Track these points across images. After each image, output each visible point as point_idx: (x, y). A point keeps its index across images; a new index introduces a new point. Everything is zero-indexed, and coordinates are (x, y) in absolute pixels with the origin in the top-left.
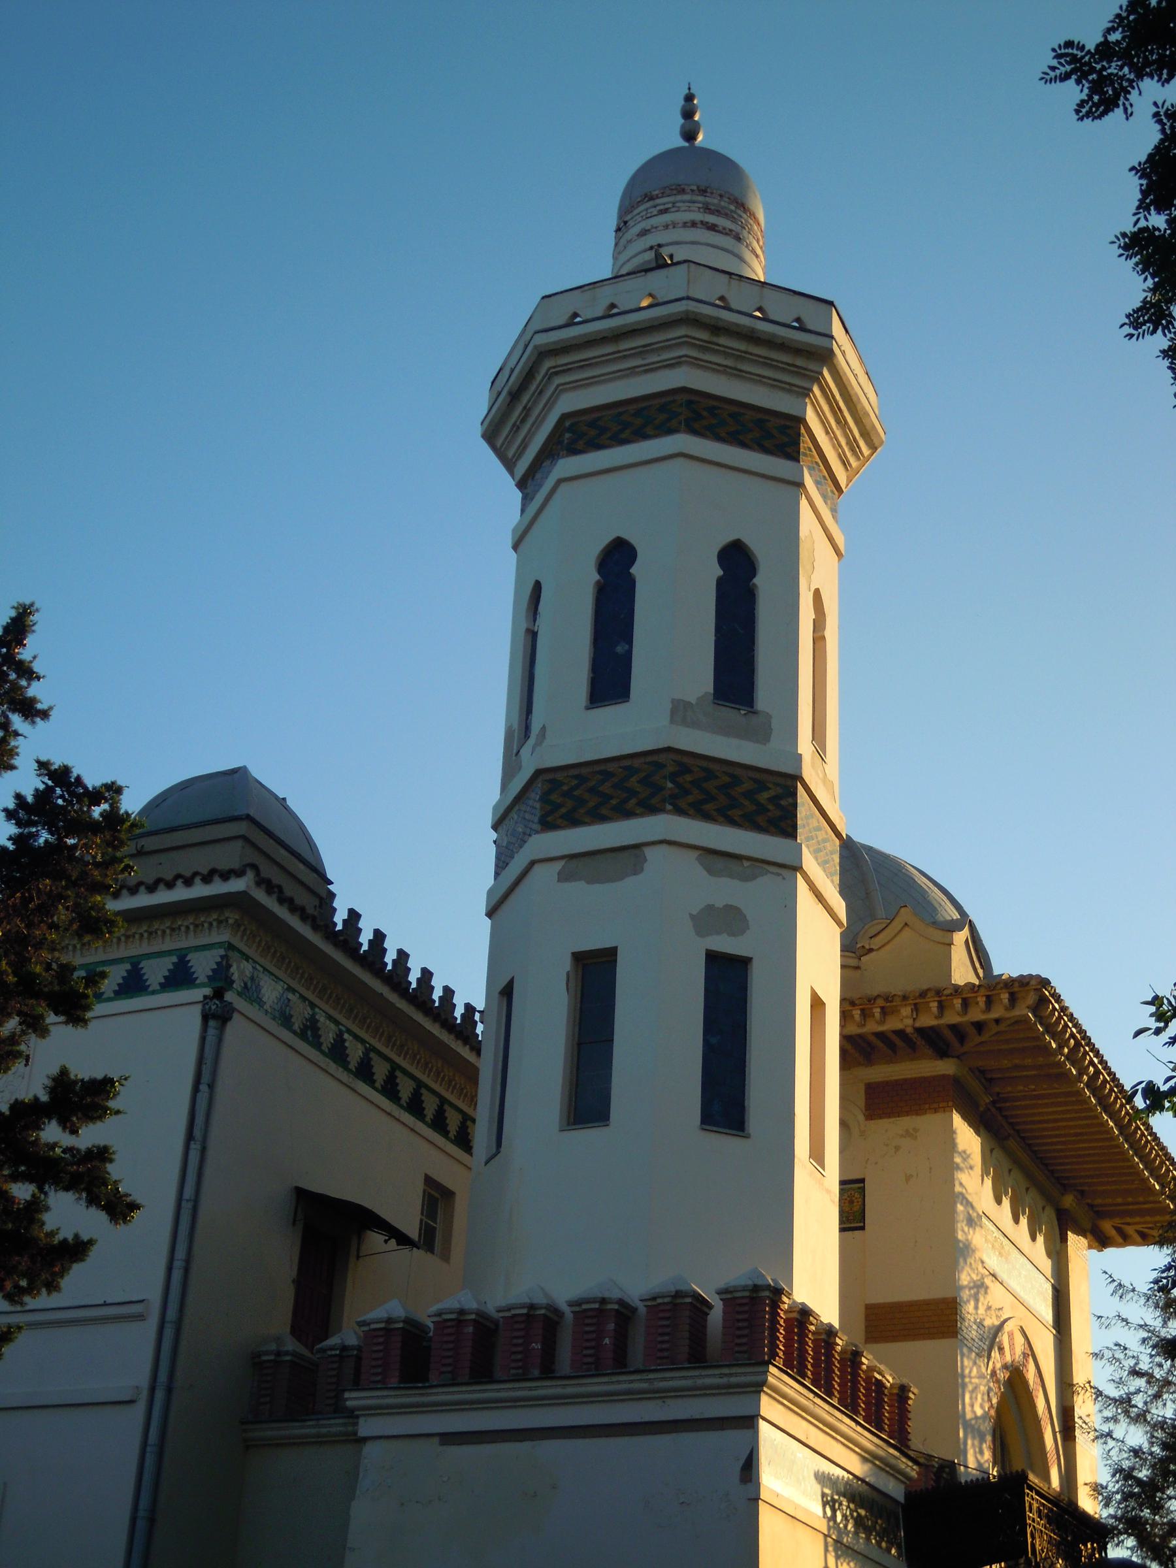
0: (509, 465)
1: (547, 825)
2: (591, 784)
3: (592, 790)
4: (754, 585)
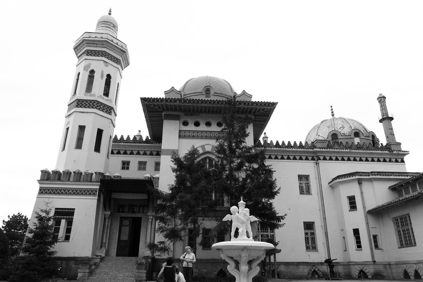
0: (77, 54)
1: (77, 106)
2: (84, 102)
3: (85, 103)
4: (111, 81)
